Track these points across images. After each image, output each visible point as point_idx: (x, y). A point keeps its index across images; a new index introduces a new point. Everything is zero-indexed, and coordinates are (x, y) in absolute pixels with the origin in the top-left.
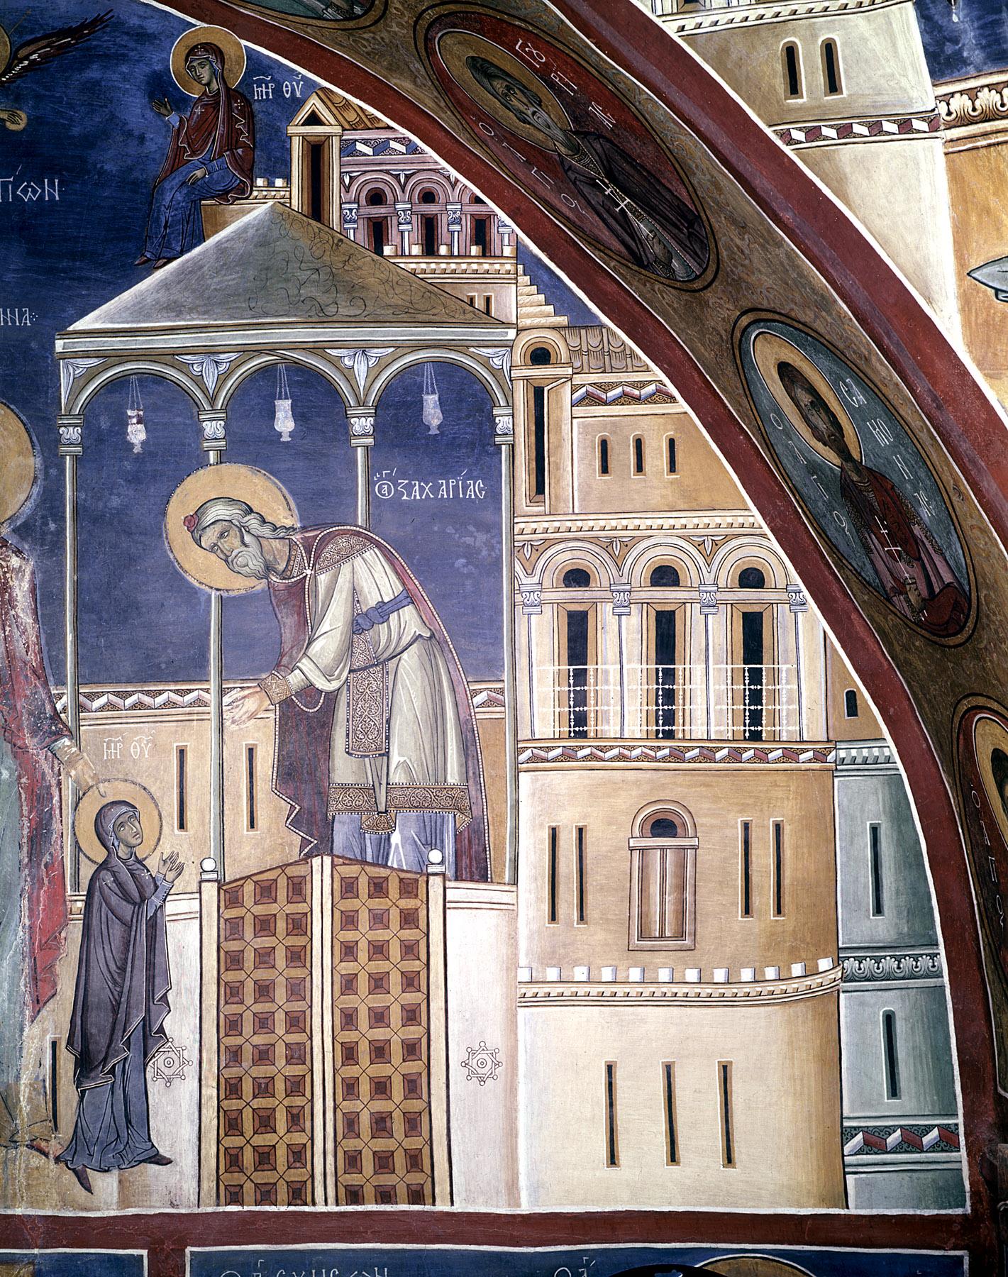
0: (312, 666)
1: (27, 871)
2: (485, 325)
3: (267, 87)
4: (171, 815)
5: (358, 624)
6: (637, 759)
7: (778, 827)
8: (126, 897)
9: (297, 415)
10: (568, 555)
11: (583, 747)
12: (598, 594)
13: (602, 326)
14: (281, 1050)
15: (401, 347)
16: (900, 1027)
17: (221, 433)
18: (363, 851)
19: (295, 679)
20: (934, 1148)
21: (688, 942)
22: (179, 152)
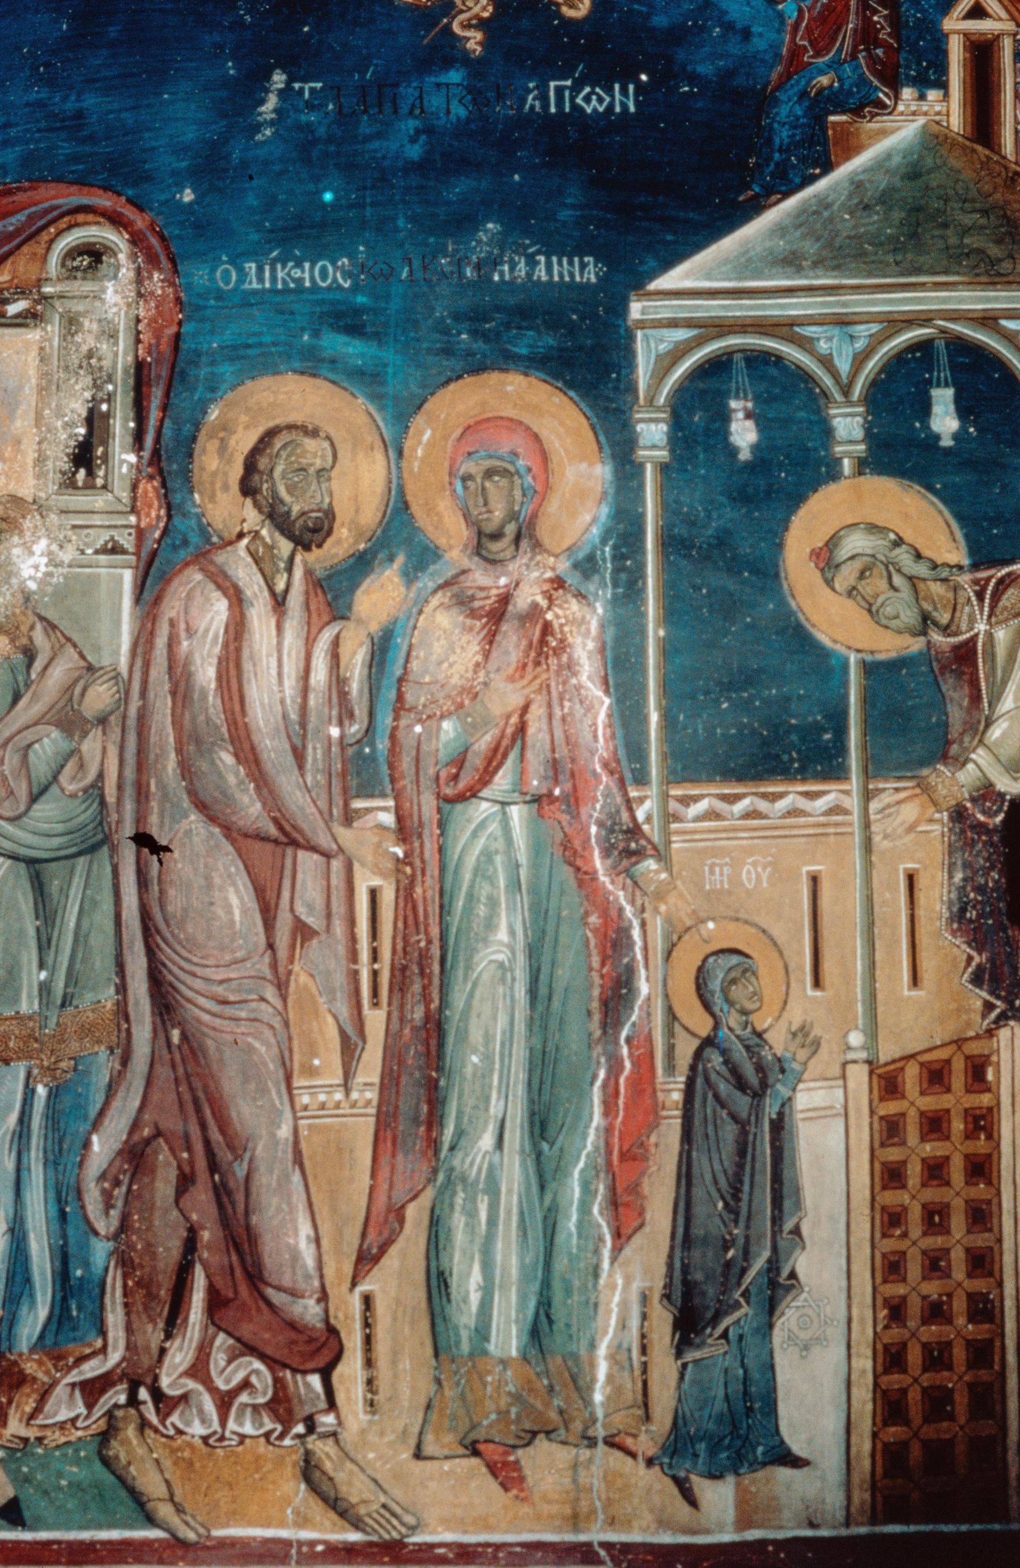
0: (990, 758)
1: (599, 1049)
4: (801, 968)
8: (741, 1084)
9: (964, 410)
14: (959, 1305)
17: (859, 434)
19: (968, 776)
22: (796, 52)
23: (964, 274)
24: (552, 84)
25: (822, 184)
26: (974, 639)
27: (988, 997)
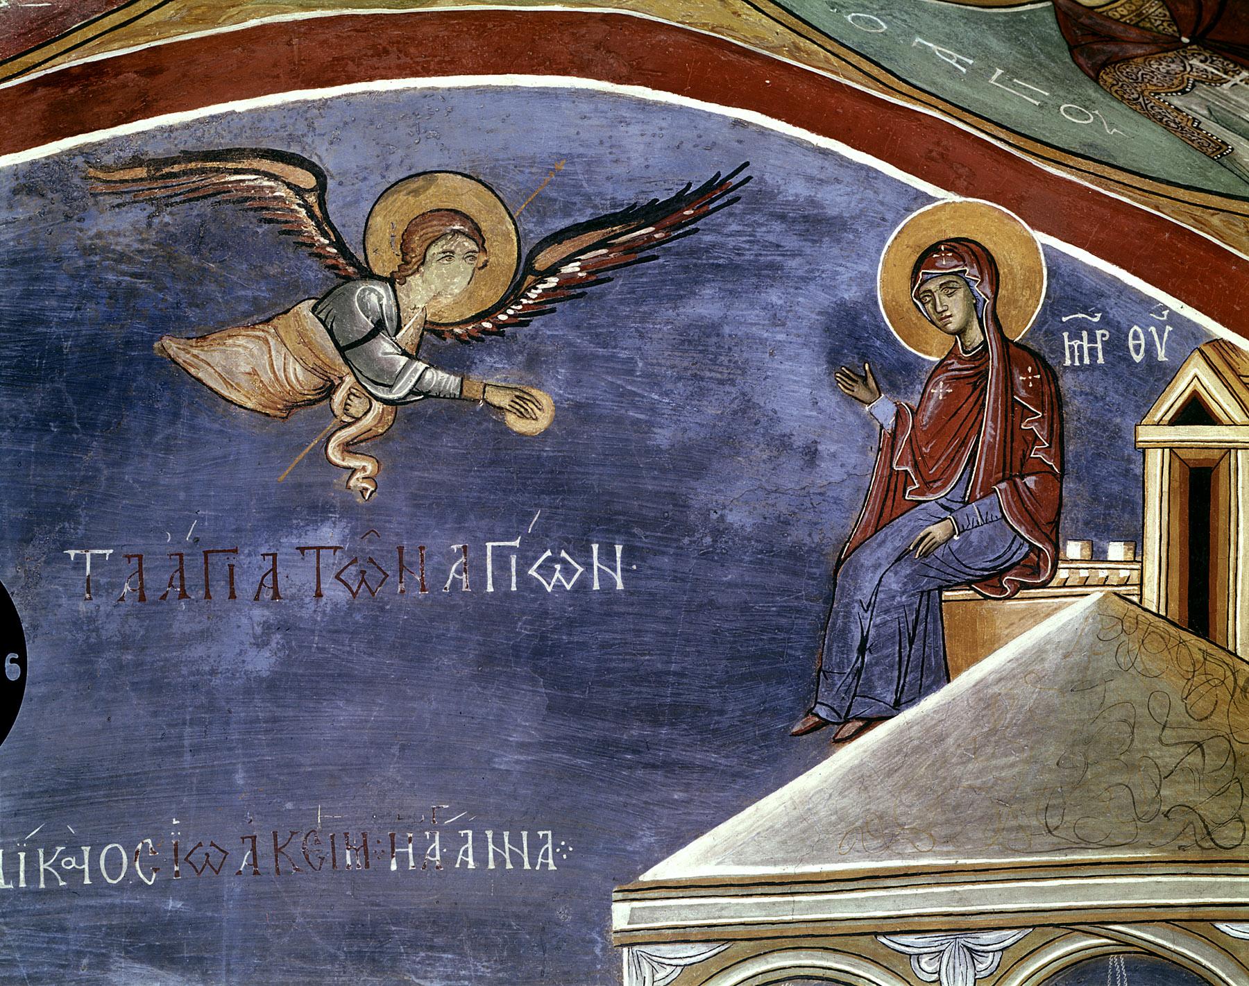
3: (1092, 339)
22: (893, 485)
23: (1159, 848)
24: (489, 545)
25: (930, 703)
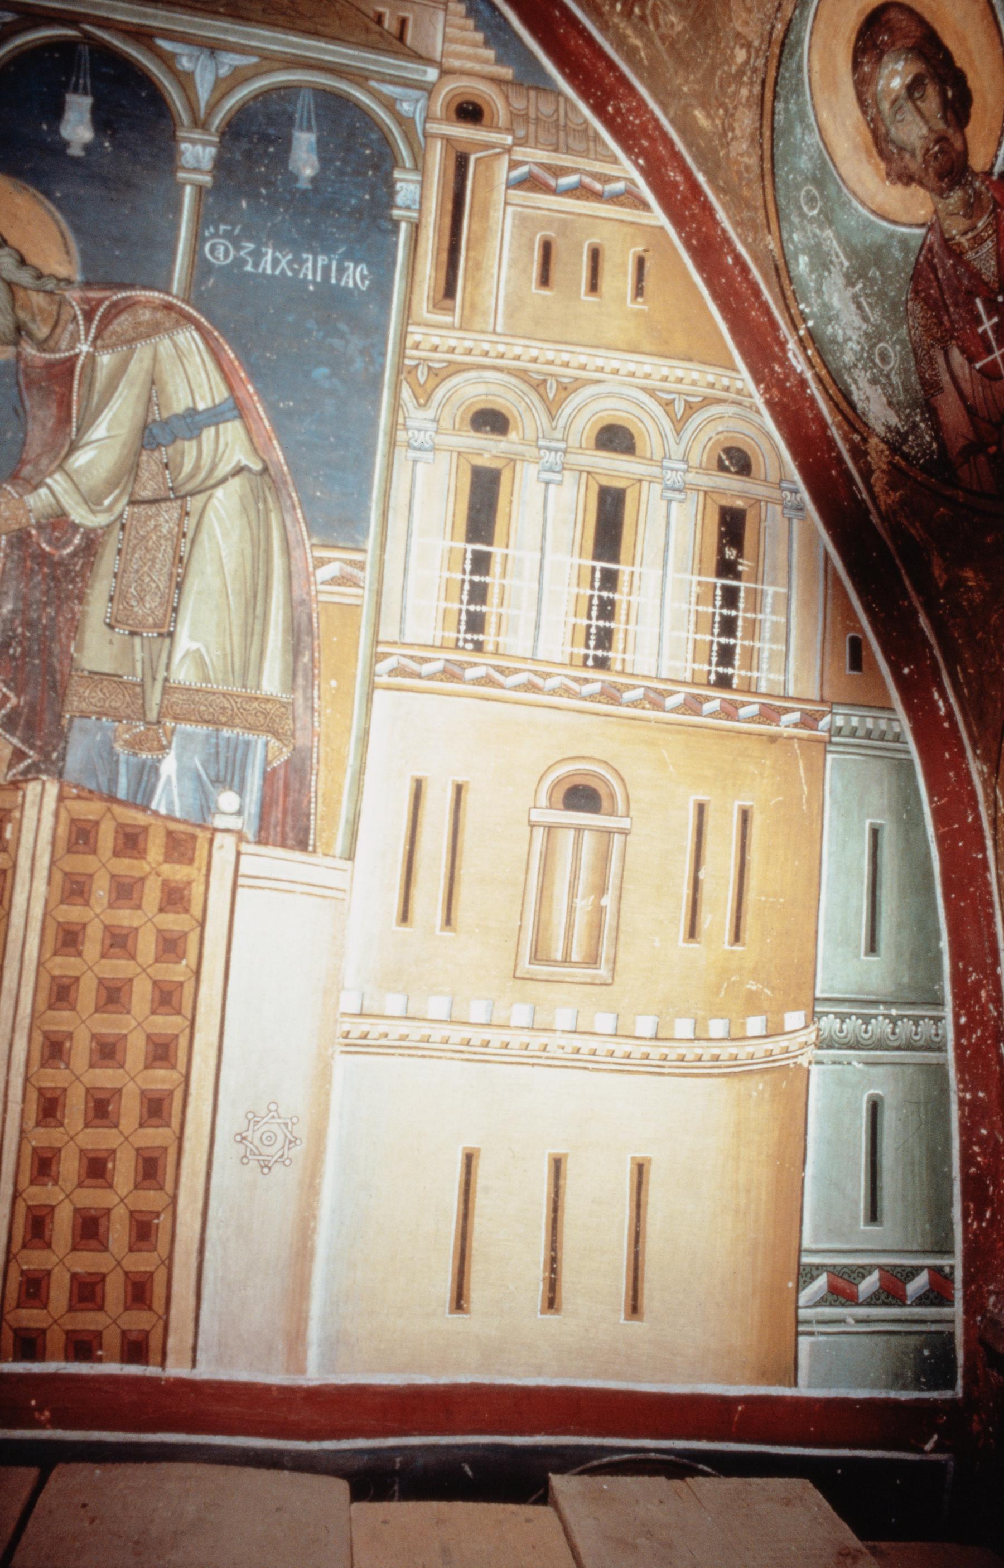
2: (395, 54)
5: (152, 435)
6: (553, 692)
7: (745, 816)
9: (101, 122)
10: (481, 389)
11: (475, 664)
12: (520, 448)
13: (559, 93)
15: (271, 61)
16: (889, 1120)
18: (113, 780)
19: (39, 500)
20: (922, 1300)
21: (603, 972)
26: (72, 360)
27: (20, 745)
